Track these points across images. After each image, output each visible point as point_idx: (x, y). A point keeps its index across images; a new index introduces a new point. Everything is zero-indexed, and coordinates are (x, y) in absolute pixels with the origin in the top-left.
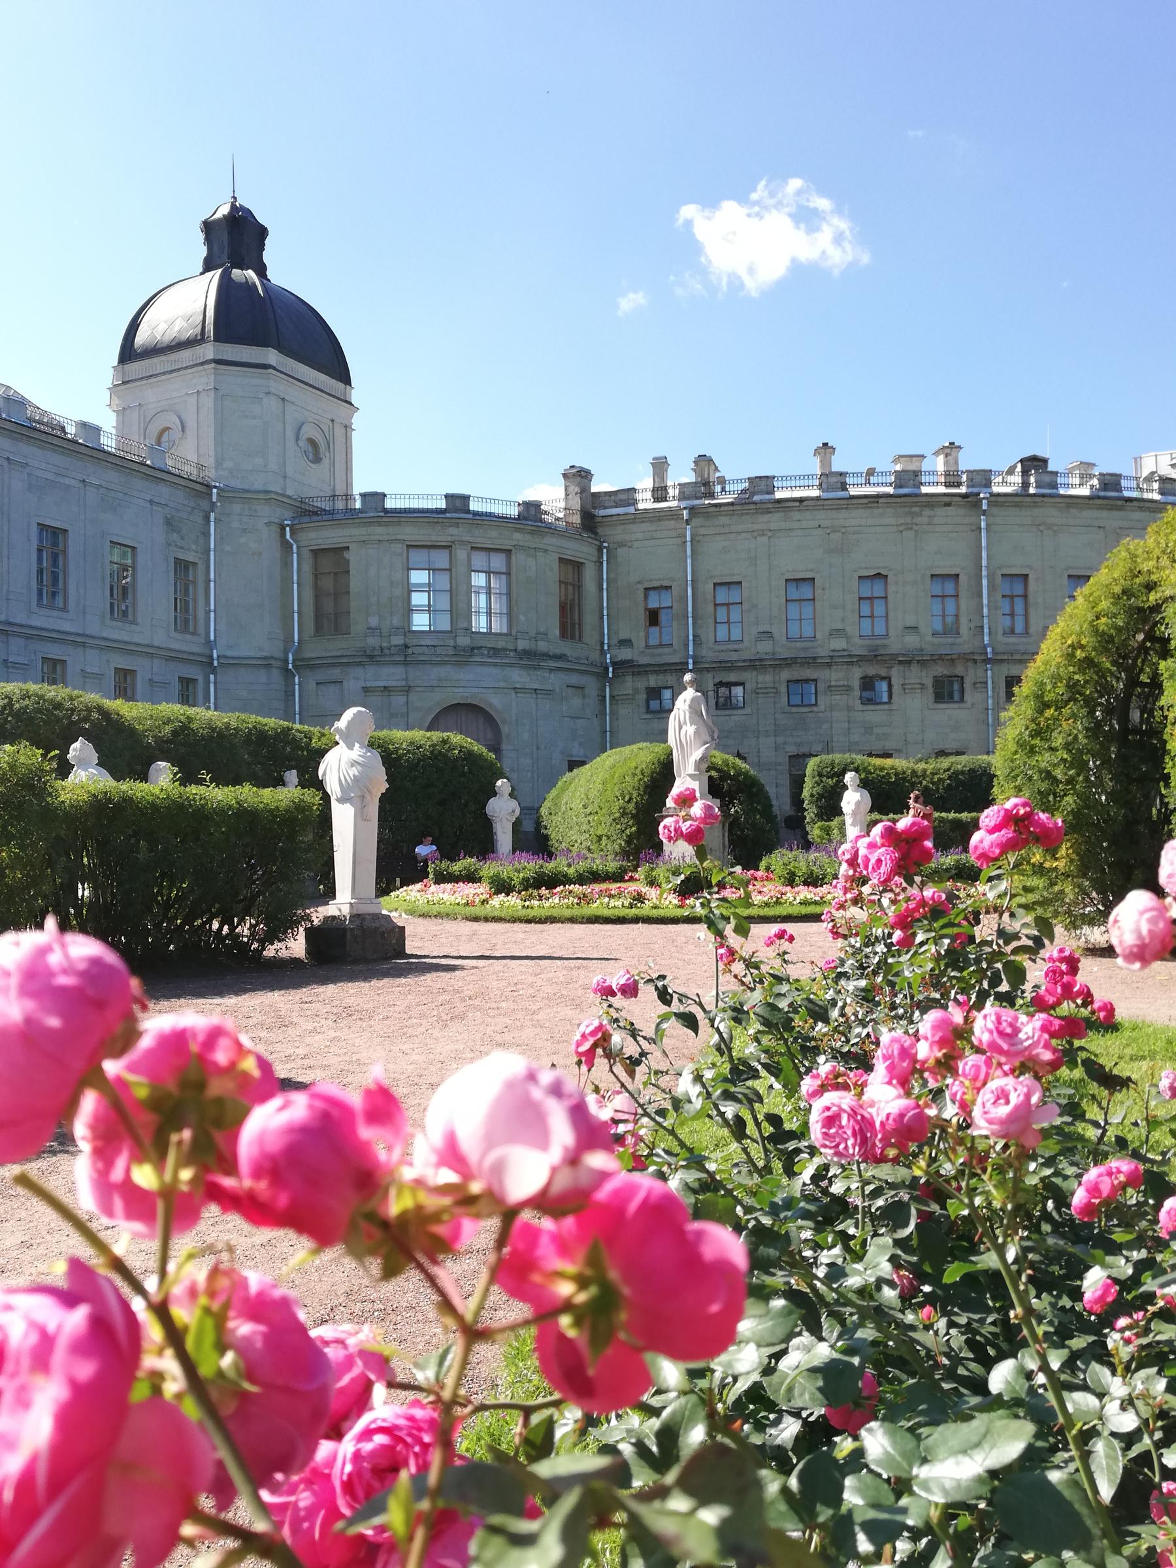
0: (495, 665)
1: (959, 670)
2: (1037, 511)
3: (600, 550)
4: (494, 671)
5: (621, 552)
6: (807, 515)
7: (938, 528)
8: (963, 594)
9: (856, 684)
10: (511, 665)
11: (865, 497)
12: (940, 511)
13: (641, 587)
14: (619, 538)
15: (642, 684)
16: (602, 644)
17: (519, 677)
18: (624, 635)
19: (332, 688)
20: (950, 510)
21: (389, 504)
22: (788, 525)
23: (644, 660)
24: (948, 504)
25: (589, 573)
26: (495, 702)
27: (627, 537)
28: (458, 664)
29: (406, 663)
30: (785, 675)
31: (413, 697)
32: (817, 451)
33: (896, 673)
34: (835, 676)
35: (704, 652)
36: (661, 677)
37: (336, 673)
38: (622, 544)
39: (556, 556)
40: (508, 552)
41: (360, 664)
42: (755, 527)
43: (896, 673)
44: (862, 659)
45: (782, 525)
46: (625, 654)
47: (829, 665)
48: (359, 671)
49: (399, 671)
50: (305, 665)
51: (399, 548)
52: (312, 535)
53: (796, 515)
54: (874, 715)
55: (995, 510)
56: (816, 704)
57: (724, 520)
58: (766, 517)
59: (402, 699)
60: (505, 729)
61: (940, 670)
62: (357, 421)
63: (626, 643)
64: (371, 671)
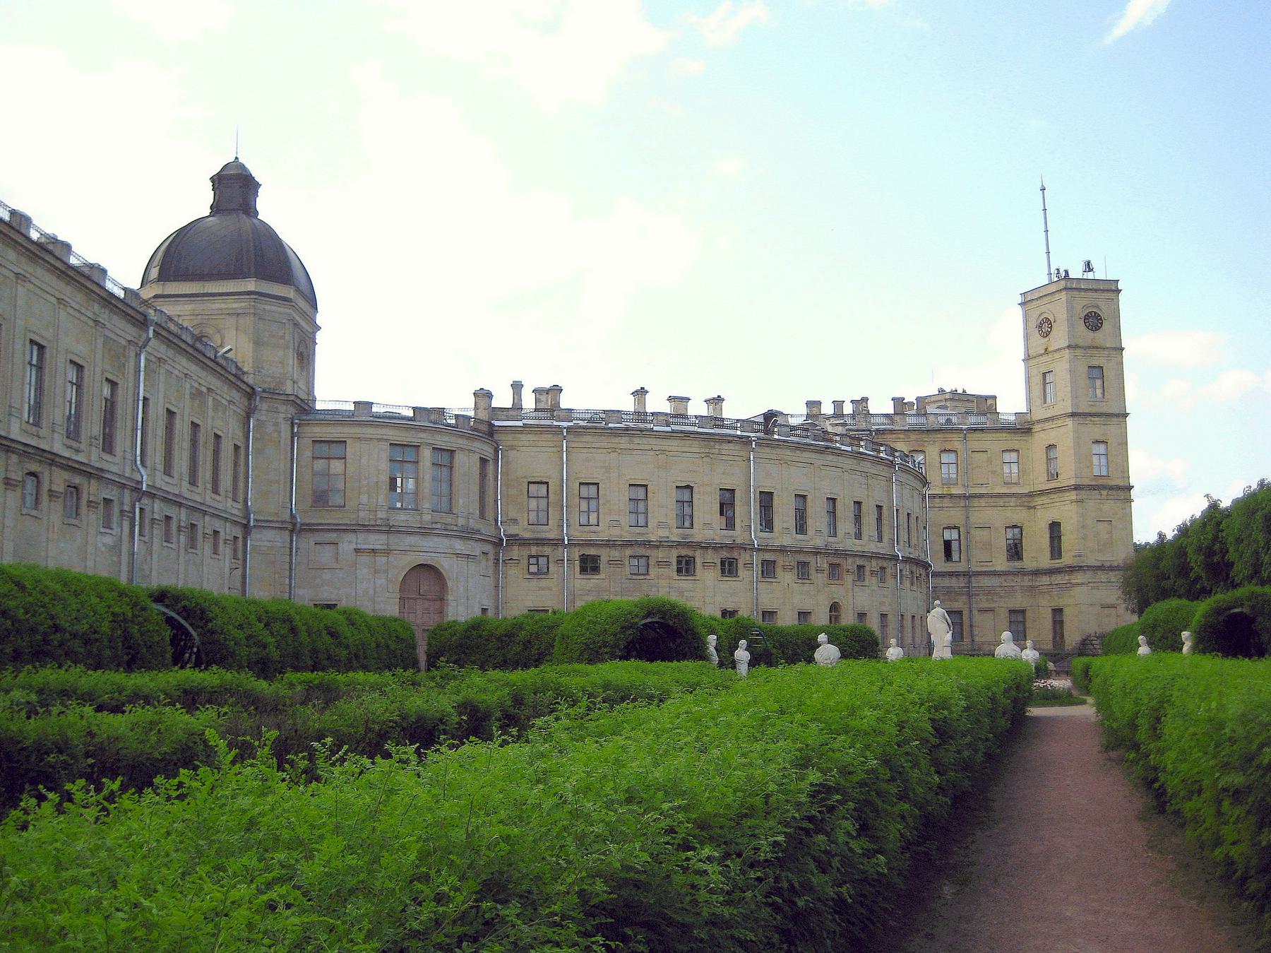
0: (447, 536)
1: (735, 555)
2: (779, 451)
3: (496, 450)
4: (446, 541)
5: (512, 453)
6: (644, 441)
7: (724, 458)
8: (737, 502)
9: (674, 561)
10: (456, 537)
11: (682, 432)
12: (725, 446)
13: (526, 481)
14: (510, 443)
15: (525, 552)
16: (496, 521)
17: (459, 546)
18: (513, 514)
19: (327, 547)
20: (731, 446)
21: (375, 409)
22: (633, 446)
23: (527, 535)
24: (729, 442)
25: (491, 467)
26: (444, 564)
27: (515, 443)
28: (423, 534)
29: (388, 532)
30: (628, 552)
31: (391, 558)
32: (635, 393)
33: (698, 555)
34: (661, 554)
35: (572, 532)
36: (540, 548)
37: (332, 536)
38: (512, 448)
39: (478, 456)
40: (452, 452)
41: (354, 531)
42: (610, 445)
43: (698, 555)
44: (679, 544)
45: (628, 446)
46: (513, 530)
47: (658, 547)
48: (352, 536)
49: (384, 537)
50: (310, 529)
51: (386, 446)
52: (317, 429)
53: (637, 440)
54: (685, 583)
55: (758, 449)
56: (647, 574)
57: (588, 438)
58: (616, 440)
59: (384, 559)
60: (450, 584)
61: (725, 554)
62: (320, 336)
63: (515, 521)
64: (361, 536)
